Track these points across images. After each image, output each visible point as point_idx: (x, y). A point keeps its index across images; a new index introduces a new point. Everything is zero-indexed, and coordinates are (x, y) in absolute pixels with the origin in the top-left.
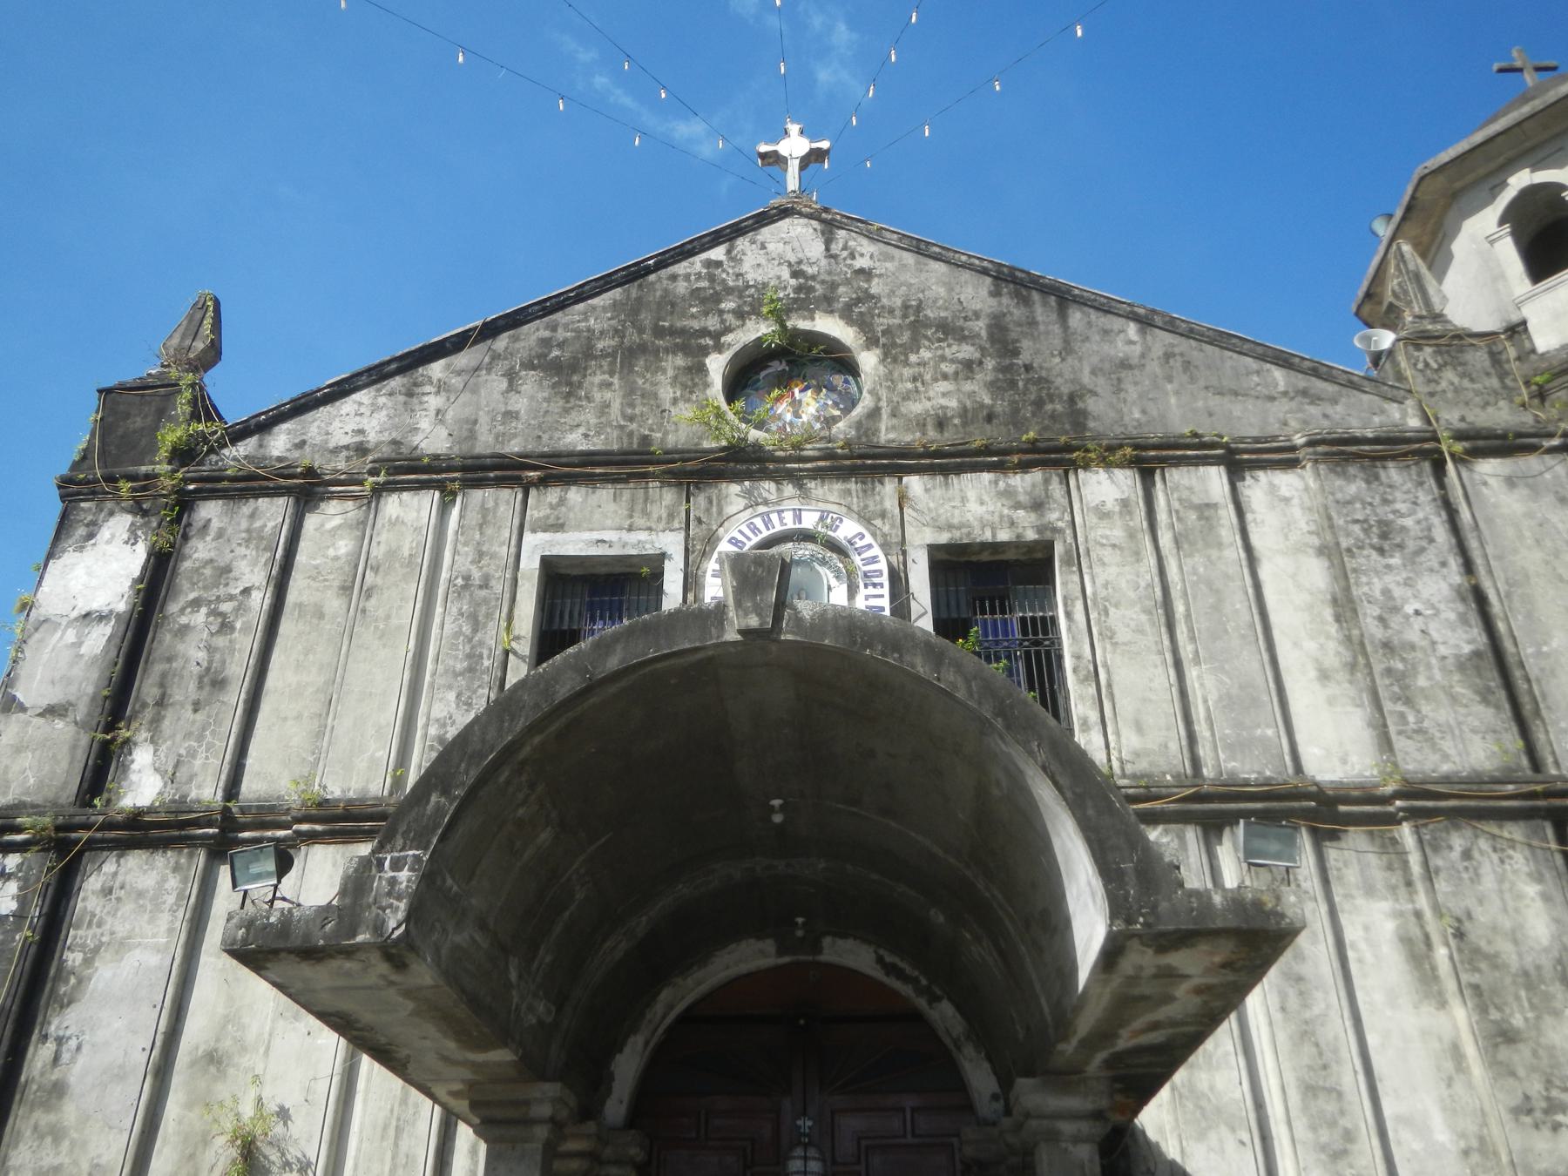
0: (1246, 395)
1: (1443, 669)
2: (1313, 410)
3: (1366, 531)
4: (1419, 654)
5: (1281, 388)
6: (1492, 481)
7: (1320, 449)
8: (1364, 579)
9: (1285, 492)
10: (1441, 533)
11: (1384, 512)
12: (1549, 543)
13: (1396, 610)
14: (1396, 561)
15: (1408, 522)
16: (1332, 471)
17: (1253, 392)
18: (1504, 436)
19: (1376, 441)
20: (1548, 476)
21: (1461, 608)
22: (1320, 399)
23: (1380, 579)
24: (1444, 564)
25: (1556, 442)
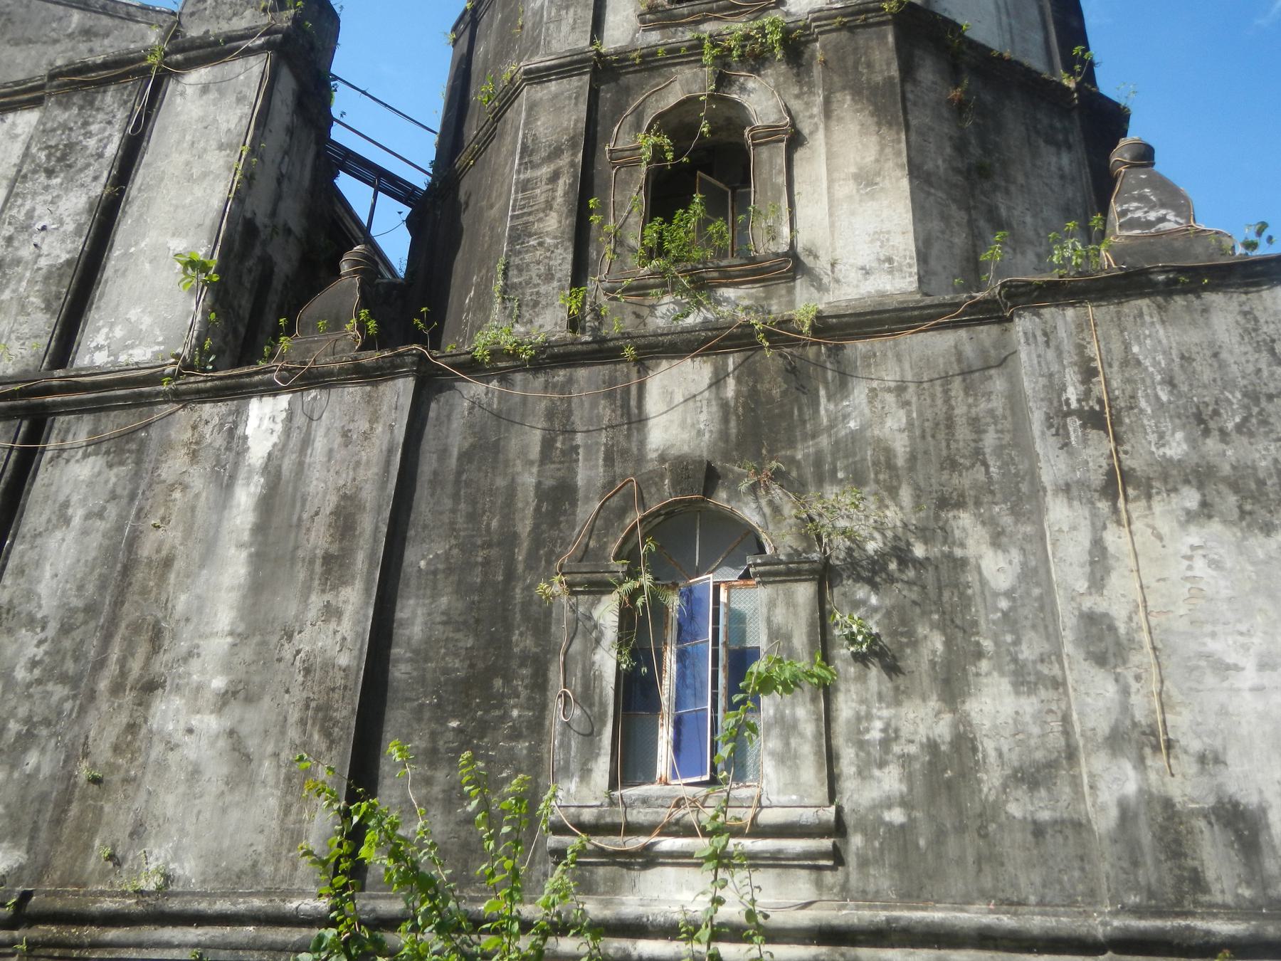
0: (36, 42)
1: (32, 282)
2: (83, 47)
3: (48, 157)
4: (20, 269)
5: (70, 30)
6: (189, 90)
7: (55, 83)
8: (20, 201)
9: (19, 130)
10: (112, 149)
11: (77, 136)
12: (202, 144)
13: (25, 228)
14: (56, 181)
15: (92, 143)
16: (59, 103)
17: (45, 39)
18: (216, 43)
19: (105, 65)
20: (242, 77)
21: (84, 218)
22: (96, 35)
23: (33, 199)
24: (96, 178)
25: (259, 42)
